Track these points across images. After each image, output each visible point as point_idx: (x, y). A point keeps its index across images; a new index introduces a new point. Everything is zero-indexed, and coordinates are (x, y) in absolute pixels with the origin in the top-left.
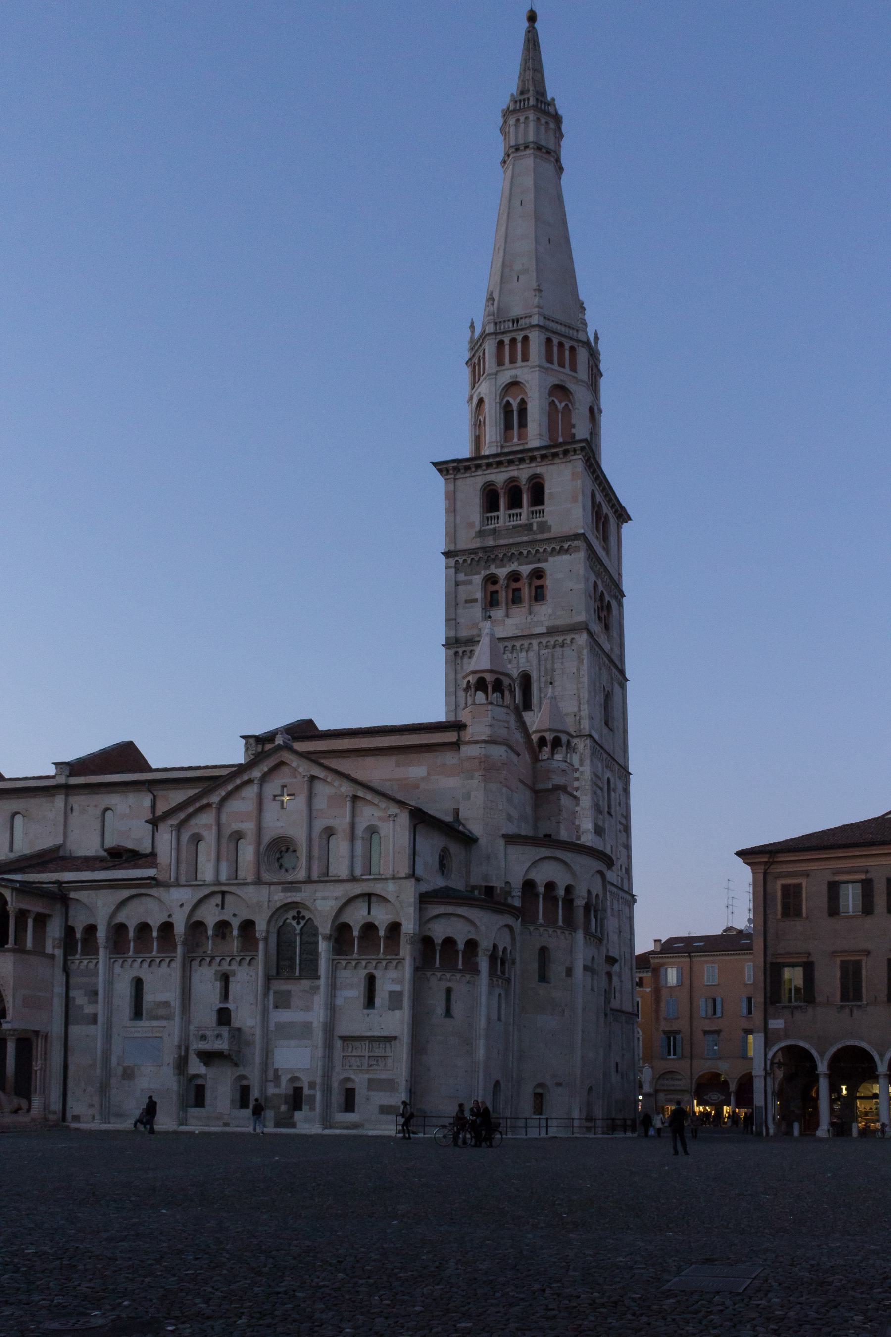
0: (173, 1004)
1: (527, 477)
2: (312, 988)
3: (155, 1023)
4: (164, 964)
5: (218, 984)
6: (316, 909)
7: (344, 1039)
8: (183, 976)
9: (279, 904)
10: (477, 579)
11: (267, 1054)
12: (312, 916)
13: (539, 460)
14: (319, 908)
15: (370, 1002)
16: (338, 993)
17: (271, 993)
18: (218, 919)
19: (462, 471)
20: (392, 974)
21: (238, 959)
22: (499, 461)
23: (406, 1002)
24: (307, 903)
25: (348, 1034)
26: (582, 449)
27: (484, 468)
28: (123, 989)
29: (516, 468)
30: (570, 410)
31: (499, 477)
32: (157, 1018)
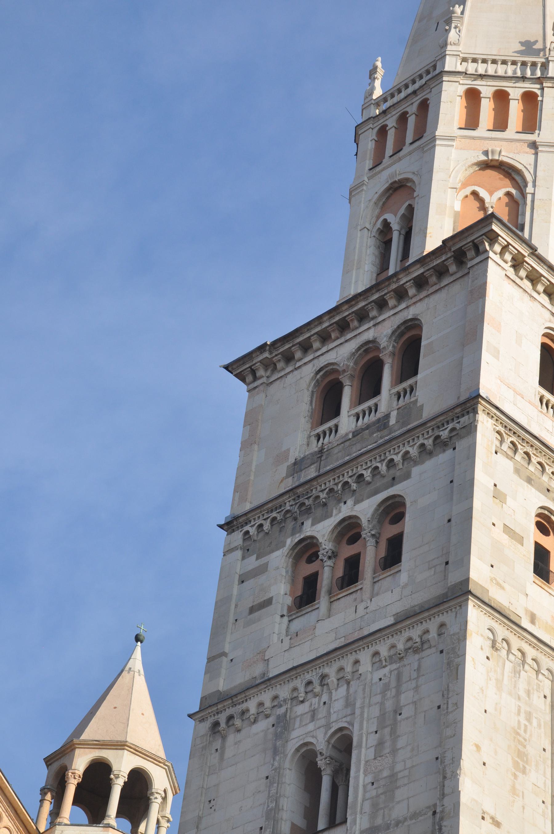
1: (390, 331)
10: (279, 559)
31: (341, 353)
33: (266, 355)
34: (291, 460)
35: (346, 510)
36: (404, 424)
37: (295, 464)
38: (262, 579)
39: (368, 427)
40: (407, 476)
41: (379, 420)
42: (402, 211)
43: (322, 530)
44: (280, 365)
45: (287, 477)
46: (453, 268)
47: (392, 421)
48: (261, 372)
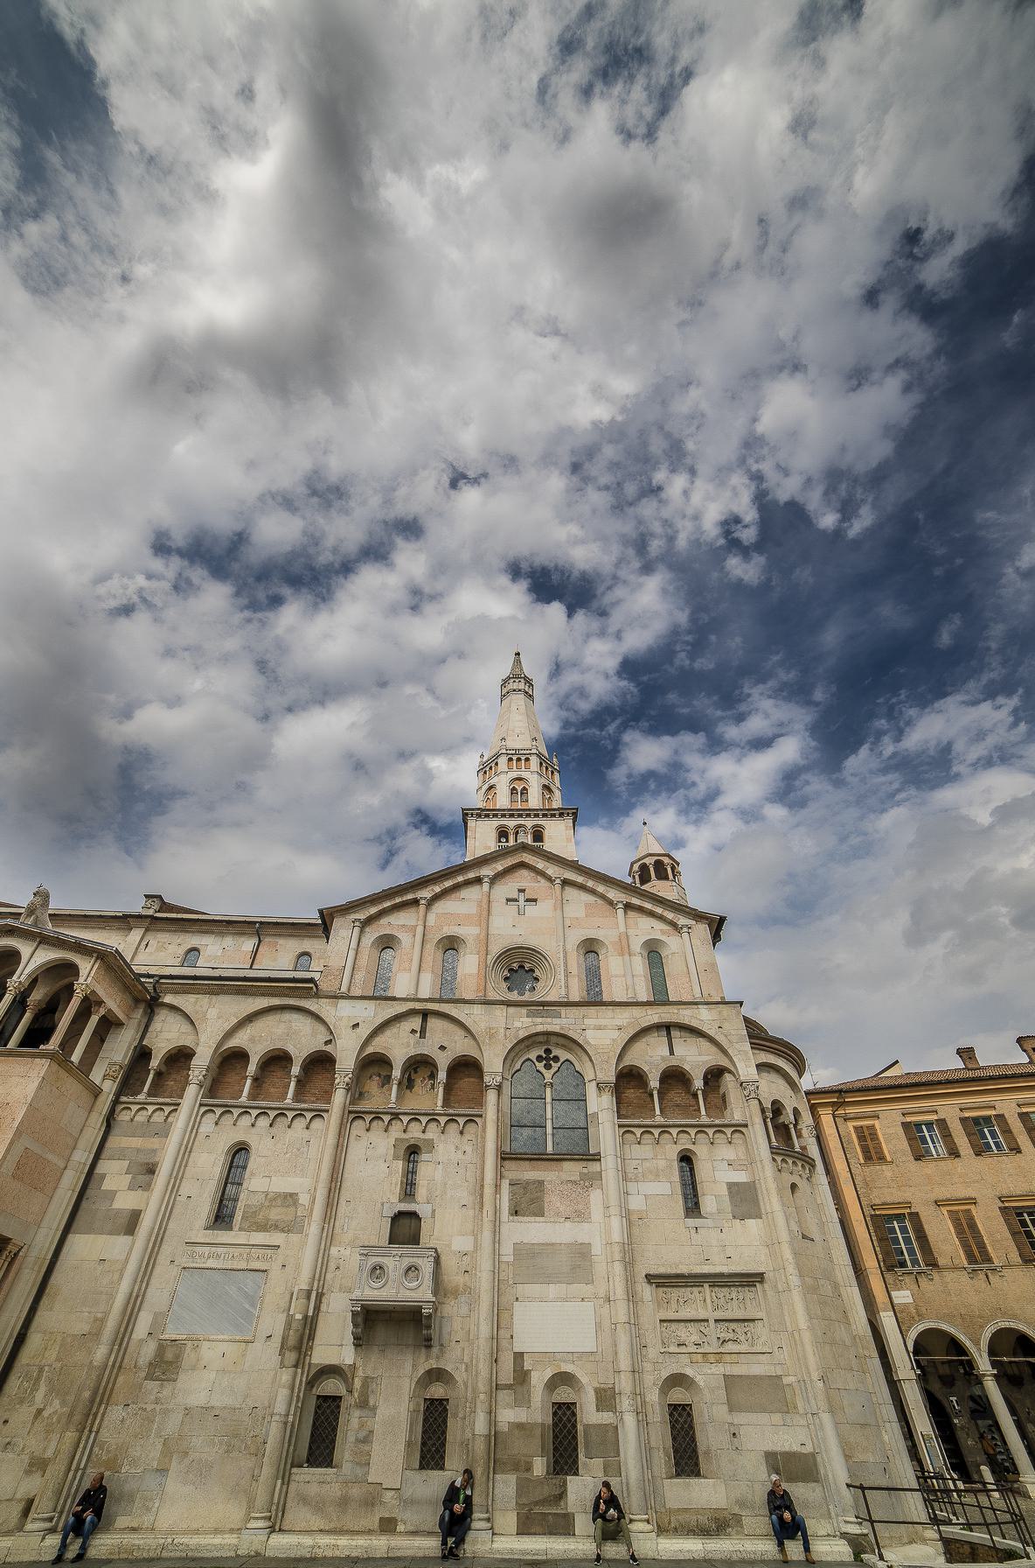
0: (304, 1199)
2: (584, 1177)
3: (259, 1238)
4: (300, 1124)
5: (399, 1165)
7: (660, 1281)
9: (522, 1034)
11: (501, 1316)
12: (569, 1056)
15: (693, 1207)
17: (505, 1184)
20: (725, 1152)
21: (443, 1120)
22: (511, 813)
24: (571, 1034)
25: (662, 1270)
28: (209, 1163)
32: (263, 1227)
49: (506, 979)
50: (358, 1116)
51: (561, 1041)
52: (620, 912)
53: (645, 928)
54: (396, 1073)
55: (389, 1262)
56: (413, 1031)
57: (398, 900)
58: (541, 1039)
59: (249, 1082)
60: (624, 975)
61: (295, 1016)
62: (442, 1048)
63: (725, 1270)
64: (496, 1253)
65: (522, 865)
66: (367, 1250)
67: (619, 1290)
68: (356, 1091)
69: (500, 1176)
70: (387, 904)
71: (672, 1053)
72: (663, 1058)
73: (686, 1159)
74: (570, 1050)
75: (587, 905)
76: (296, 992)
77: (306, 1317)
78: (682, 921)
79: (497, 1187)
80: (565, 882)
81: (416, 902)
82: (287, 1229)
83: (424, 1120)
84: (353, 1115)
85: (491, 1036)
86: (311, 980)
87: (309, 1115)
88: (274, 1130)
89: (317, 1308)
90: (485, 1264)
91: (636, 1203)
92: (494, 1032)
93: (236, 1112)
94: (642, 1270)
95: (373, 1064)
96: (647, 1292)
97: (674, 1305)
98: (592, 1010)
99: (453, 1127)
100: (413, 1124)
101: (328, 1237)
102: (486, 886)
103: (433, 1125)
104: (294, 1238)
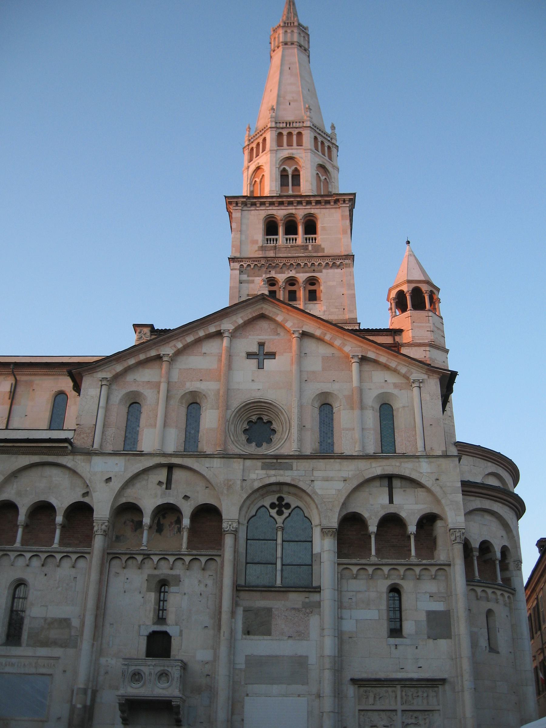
0: (75, 623)
1: (303, 214)
2: (306, 605)
3: (42, 652)
4: (66, 563)
5: (152, 596)
6: (315, 493)
8: (100, 582)
9: (257, 485)
12: (300, 504)
13: (314, 204)
14: (319, 492)
16: (346, 613)
17: (240, 611)
18: (160, 501)
19: (249, 206)
20: (430, 586)
21: (187, 559)
23: (461, 628)
24: (301, 485)
25: (364, 676)
26: (350, 200)
27: (267, 205)
29: (294, 208)
30: (327, 182)
31: (280, 213)
32: (45, 643)
33: (245, 200)
34: (260, 244)
35: (292, 274)
36: (315, 252)
37: (262, 247)
38: (251, 285)
39: (298, 246)
40: (321, 272)
41: (303, 246)
42: (293, 168)
43: (281, 277)
44: (249, 206)
45: (258, 250)
46: (332, 203)
47: (310, 248)
48: (240, 205)
49: (245, 431)
50: (116, 556)
51: (292, 490)
52: (355, 367)
53: (380, 382)
54: (147, 520)
55: (145, 670)
56: (160, 483)
57: (142, 357)
58: (274, 488)
59: (20, 531)
60: (354, 430)
61: (54, 472)
62: (186, 497)
63: (415, 676)
64: (231, 662)
65: (263, 317)
66: (128, 661)
67: (327, 688)
68: (114, 536)
69: (235, 604)
70: (132, 361)
71: (391, 501)
72: (383, 507)
73: (395, 590)
74: (300, 498)
75: (325, 359)
76: (50, 450)
77: (85, 706)
78: (417, 375)
79: (233, 613)
80: (304, 335)
81: (159, 358)
82: (64, 644)
83: (171, 559)
84: (110, 556)
85: (229, 487)
86: (66, 440)
87: (74, 557)
88: (45, 569)
89: (93, 700)
90: (222, 671)
91: (348, 626)
92: (230, 483)
93: (12, 555)
94: (348, 675)
95: (127, 511)
96: (351, 691)
97: (371, 700)
98: (321, 464)
99: (196, 565)
100: (163, 563)
101: (98, 651)
102: (226, 342)
103: (179, 564)
104: (71, 651)
